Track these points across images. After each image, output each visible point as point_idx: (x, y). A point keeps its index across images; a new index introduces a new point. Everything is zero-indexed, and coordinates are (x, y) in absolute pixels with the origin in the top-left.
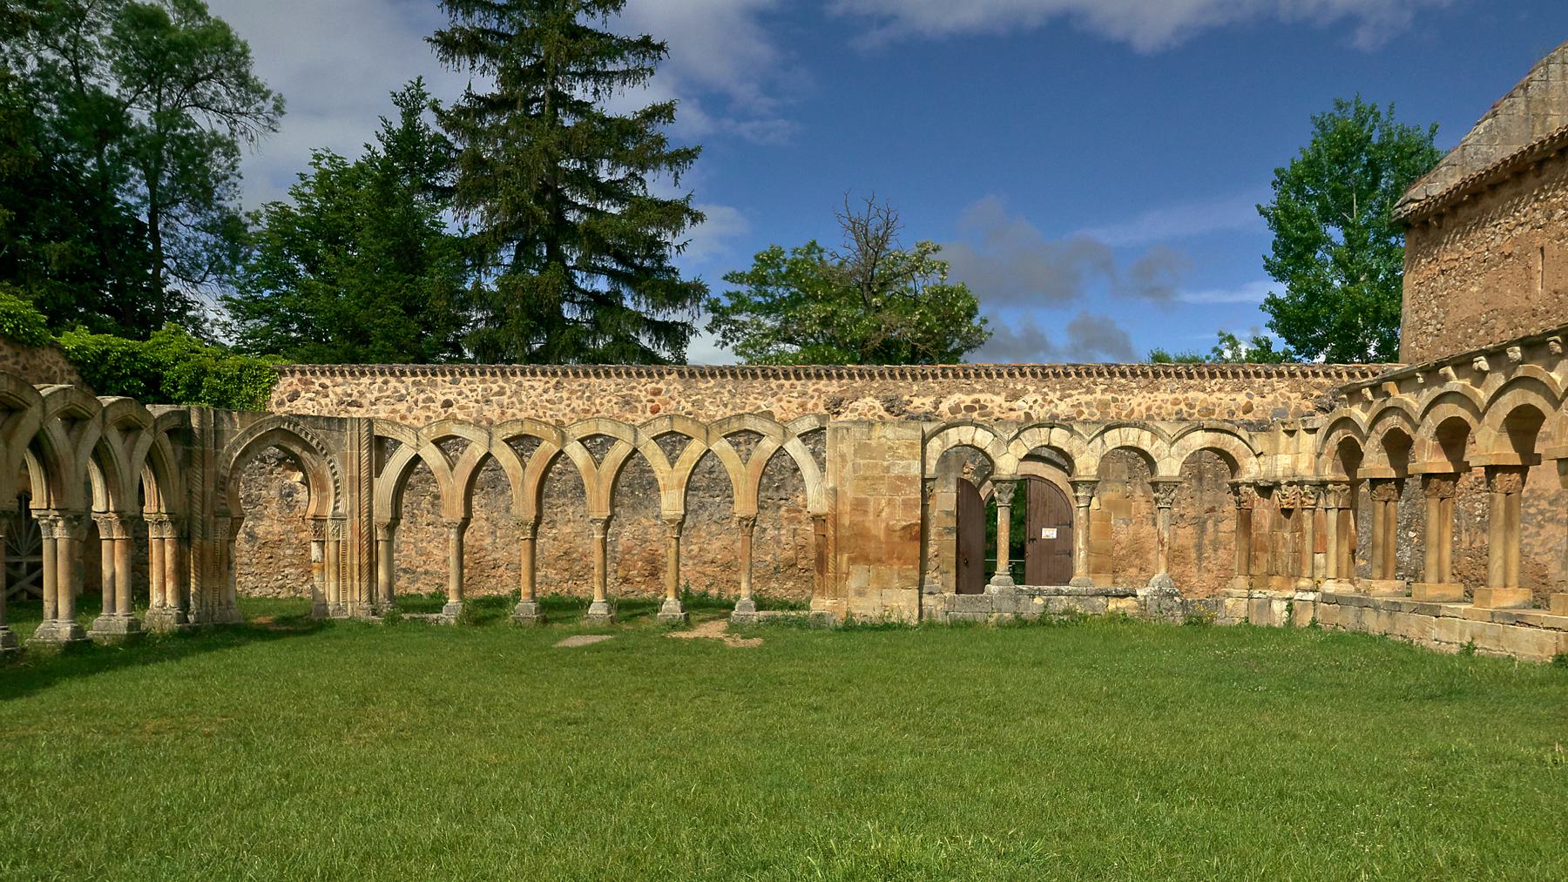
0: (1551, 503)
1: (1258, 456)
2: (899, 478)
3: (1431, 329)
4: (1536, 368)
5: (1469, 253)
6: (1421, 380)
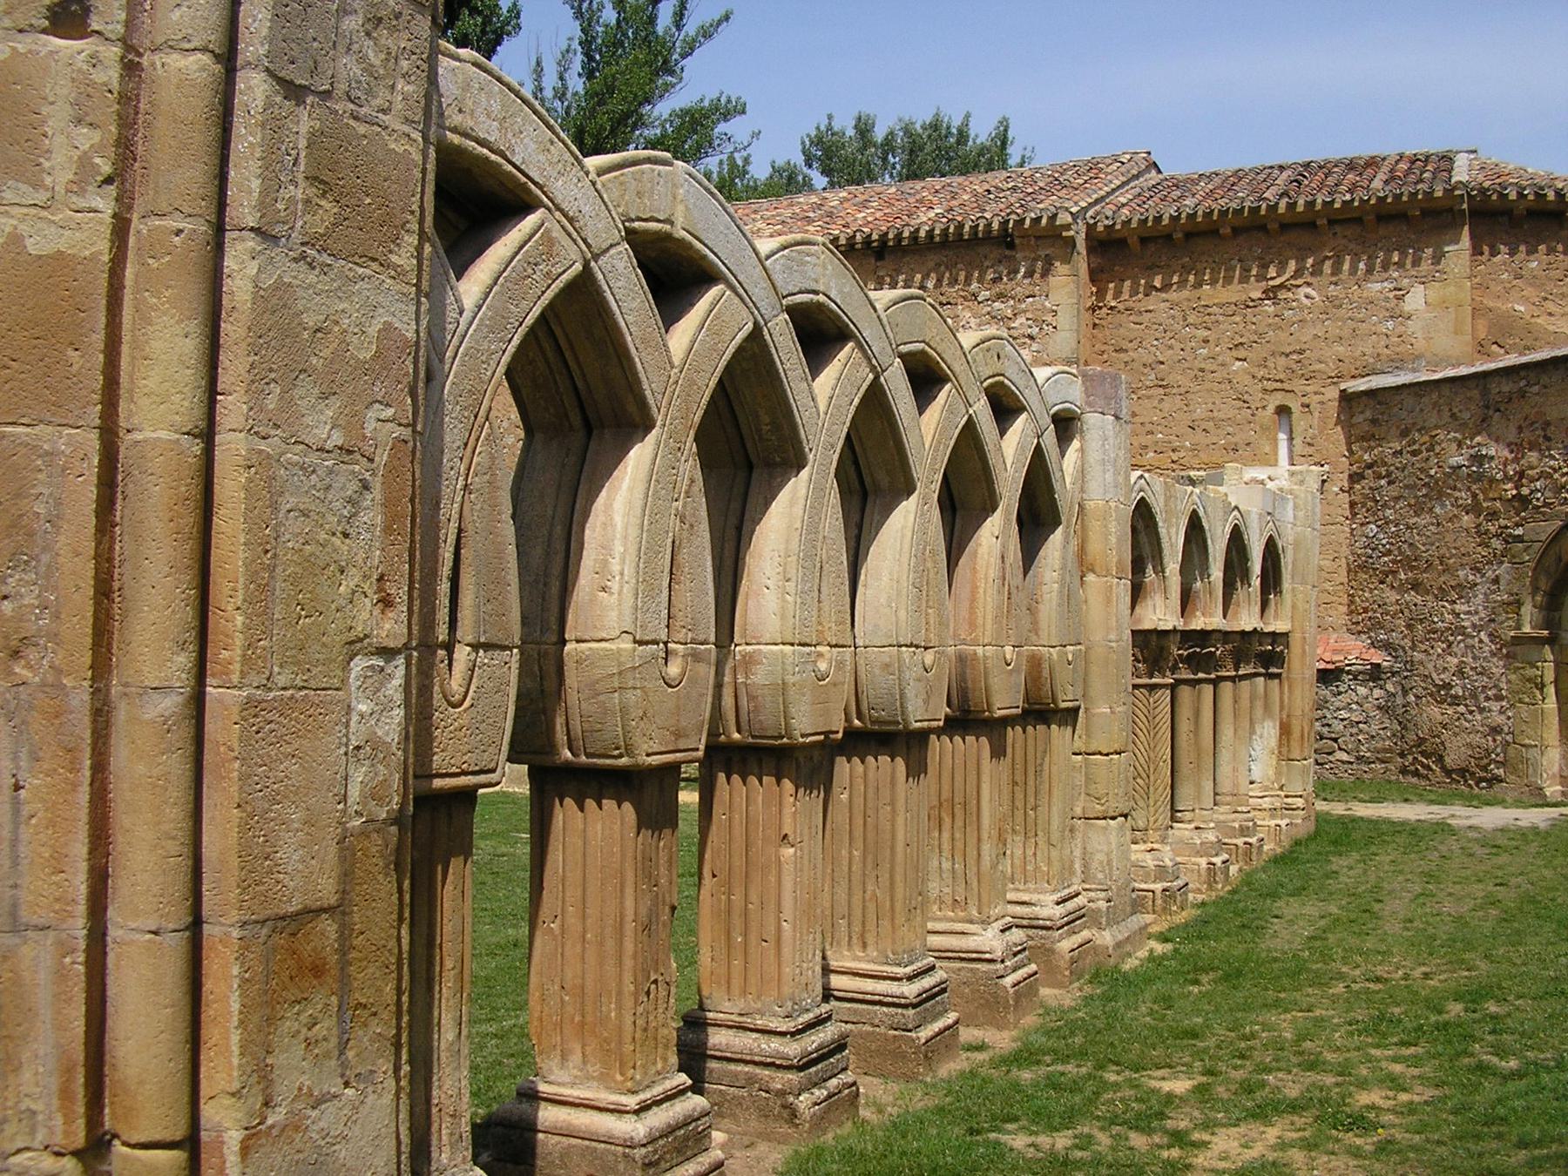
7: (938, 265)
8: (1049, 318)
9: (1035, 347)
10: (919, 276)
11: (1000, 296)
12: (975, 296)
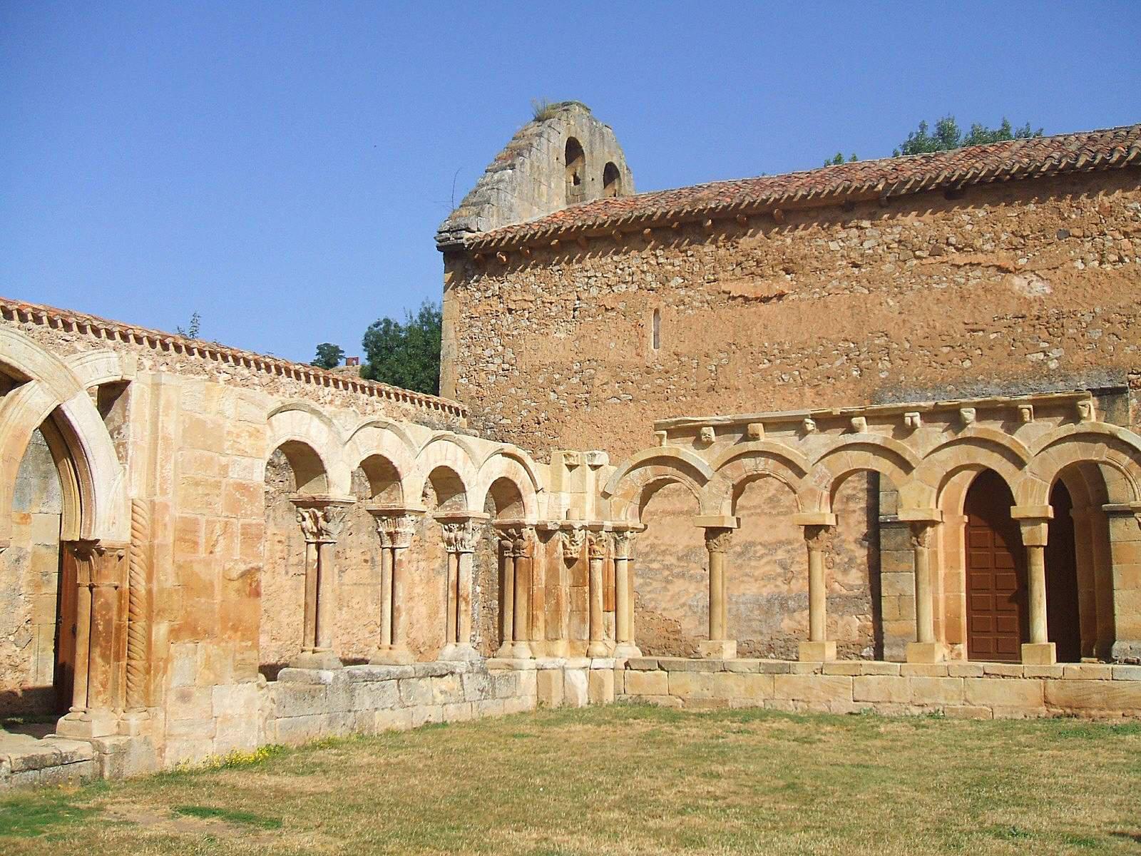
0: (679, 559)
2: (243, 488)
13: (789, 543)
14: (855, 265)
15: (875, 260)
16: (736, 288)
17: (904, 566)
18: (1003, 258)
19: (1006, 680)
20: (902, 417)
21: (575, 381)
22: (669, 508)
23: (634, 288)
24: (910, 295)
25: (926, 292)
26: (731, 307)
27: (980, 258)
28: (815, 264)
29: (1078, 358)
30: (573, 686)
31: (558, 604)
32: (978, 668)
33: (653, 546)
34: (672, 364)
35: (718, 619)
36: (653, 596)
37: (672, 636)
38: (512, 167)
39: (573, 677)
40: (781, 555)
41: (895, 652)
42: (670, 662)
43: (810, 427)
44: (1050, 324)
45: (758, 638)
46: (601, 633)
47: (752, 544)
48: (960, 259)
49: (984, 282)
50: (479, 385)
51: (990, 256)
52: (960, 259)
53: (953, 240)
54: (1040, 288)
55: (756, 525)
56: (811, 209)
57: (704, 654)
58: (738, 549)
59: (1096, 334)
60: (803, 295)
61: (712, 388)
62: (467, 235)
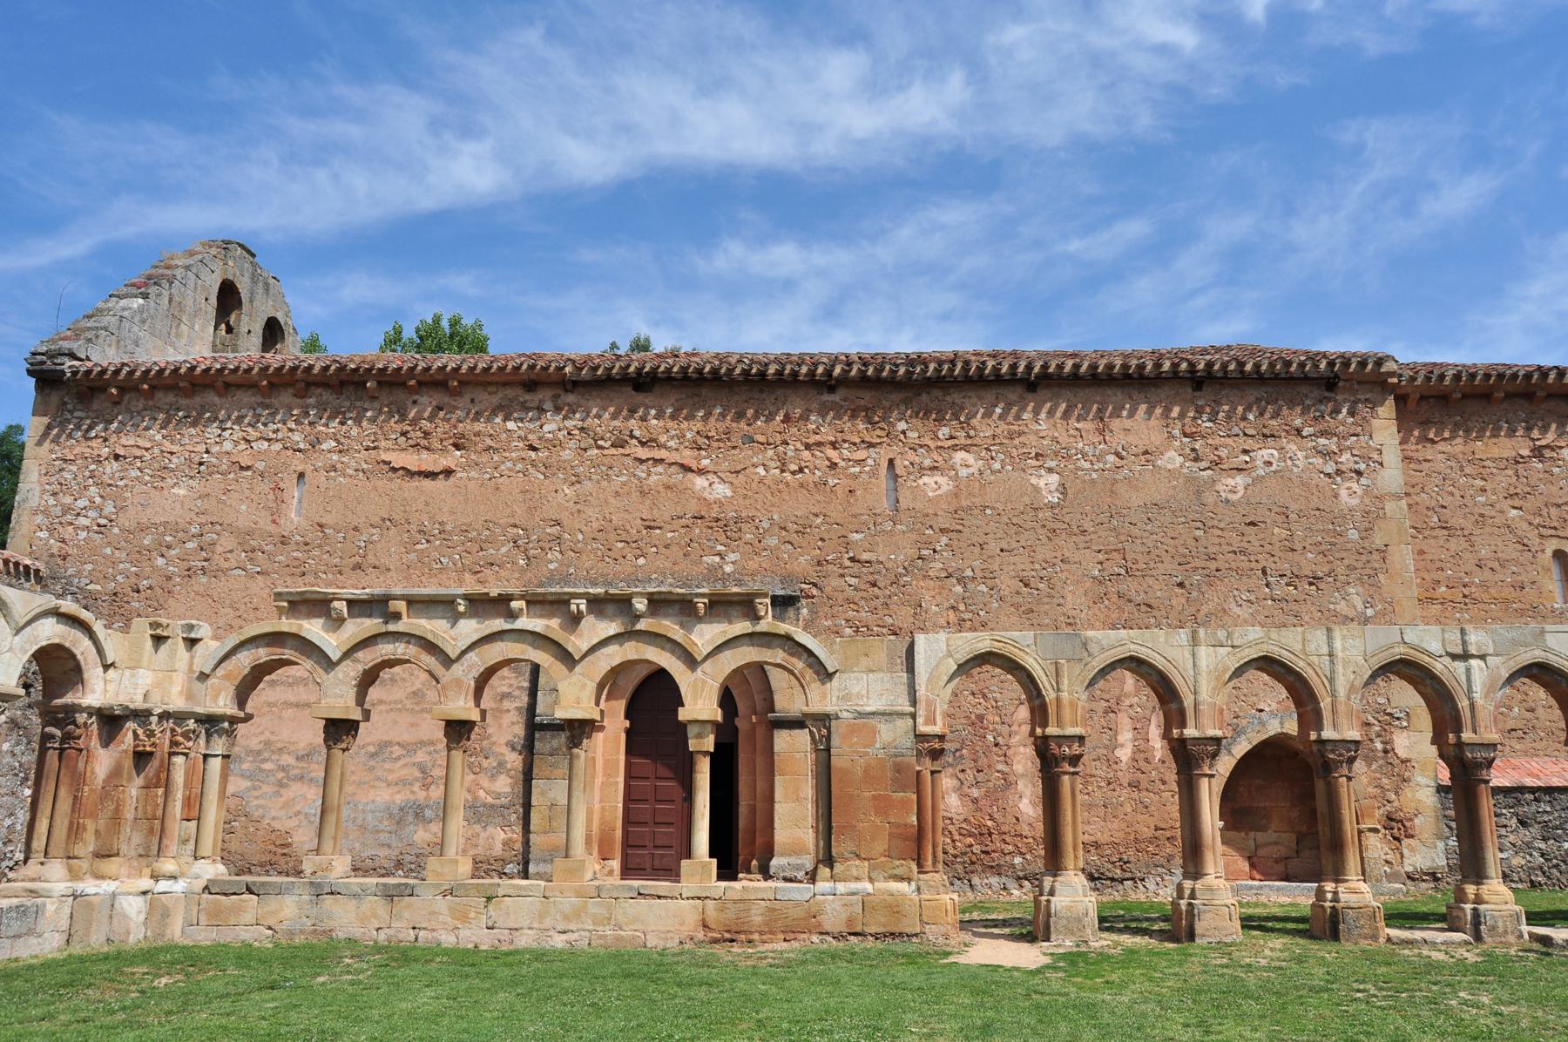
1: (106, 667)
3: (83, 521)
4: (670, 626)
5: (168, 446)
6: (461, 609)
7: (1258, 400)
8: (1375, 456)
9: (1363, 481)
10: (1240, 409)
11: (1323, 433)
12: (1299, 431)
13: (432, 743)
14: (534, 449)
15: (555, 444)
16: (398, 459)
17: (558, 772)
18: (687, 456)
19: (662, 901)
20: (567, 603)
21: (190, 545)
22: (292, 698)
23: (277, 446)
24: (588, 485)
25: (605, 483)
26: (391, 479)
27: (662, 454)
28: (489, 442)
29: (752, 565)
30: (125, 916)
31: (117, 810)
32: (631, 888)
33: (268, 743)
34: (314, 536)
35: (330, 830)
36: (261, 802)
37: (280, 851)
38: (145, 296)
39: (125, 905)
40: (421, 756)
41: (543, 868)
42: (263, 884)
43: (461, 609)
44: (725, 526)
45: (383, 852)
46: (172, 846)
47: (388, 744)
48: (643, 453)
49: (665, 479)
50: (63, 541)
51: (674, 454)
52: (643, 453)
53: (637, 433)
54: (722, 490)
55: (395, 722)
56: (490, 384)
57: (308, 871)
58: (371, 749)
59: (772, 541)
60: (473, 474)
61: (357, 567)
62: (69, 363)
